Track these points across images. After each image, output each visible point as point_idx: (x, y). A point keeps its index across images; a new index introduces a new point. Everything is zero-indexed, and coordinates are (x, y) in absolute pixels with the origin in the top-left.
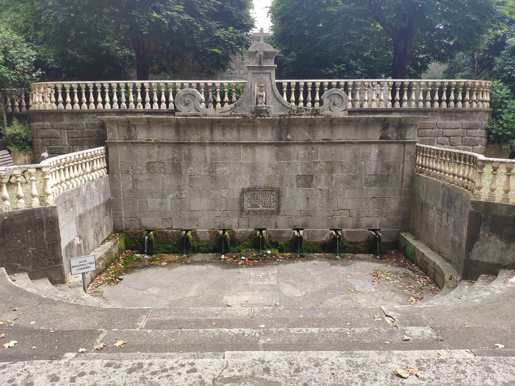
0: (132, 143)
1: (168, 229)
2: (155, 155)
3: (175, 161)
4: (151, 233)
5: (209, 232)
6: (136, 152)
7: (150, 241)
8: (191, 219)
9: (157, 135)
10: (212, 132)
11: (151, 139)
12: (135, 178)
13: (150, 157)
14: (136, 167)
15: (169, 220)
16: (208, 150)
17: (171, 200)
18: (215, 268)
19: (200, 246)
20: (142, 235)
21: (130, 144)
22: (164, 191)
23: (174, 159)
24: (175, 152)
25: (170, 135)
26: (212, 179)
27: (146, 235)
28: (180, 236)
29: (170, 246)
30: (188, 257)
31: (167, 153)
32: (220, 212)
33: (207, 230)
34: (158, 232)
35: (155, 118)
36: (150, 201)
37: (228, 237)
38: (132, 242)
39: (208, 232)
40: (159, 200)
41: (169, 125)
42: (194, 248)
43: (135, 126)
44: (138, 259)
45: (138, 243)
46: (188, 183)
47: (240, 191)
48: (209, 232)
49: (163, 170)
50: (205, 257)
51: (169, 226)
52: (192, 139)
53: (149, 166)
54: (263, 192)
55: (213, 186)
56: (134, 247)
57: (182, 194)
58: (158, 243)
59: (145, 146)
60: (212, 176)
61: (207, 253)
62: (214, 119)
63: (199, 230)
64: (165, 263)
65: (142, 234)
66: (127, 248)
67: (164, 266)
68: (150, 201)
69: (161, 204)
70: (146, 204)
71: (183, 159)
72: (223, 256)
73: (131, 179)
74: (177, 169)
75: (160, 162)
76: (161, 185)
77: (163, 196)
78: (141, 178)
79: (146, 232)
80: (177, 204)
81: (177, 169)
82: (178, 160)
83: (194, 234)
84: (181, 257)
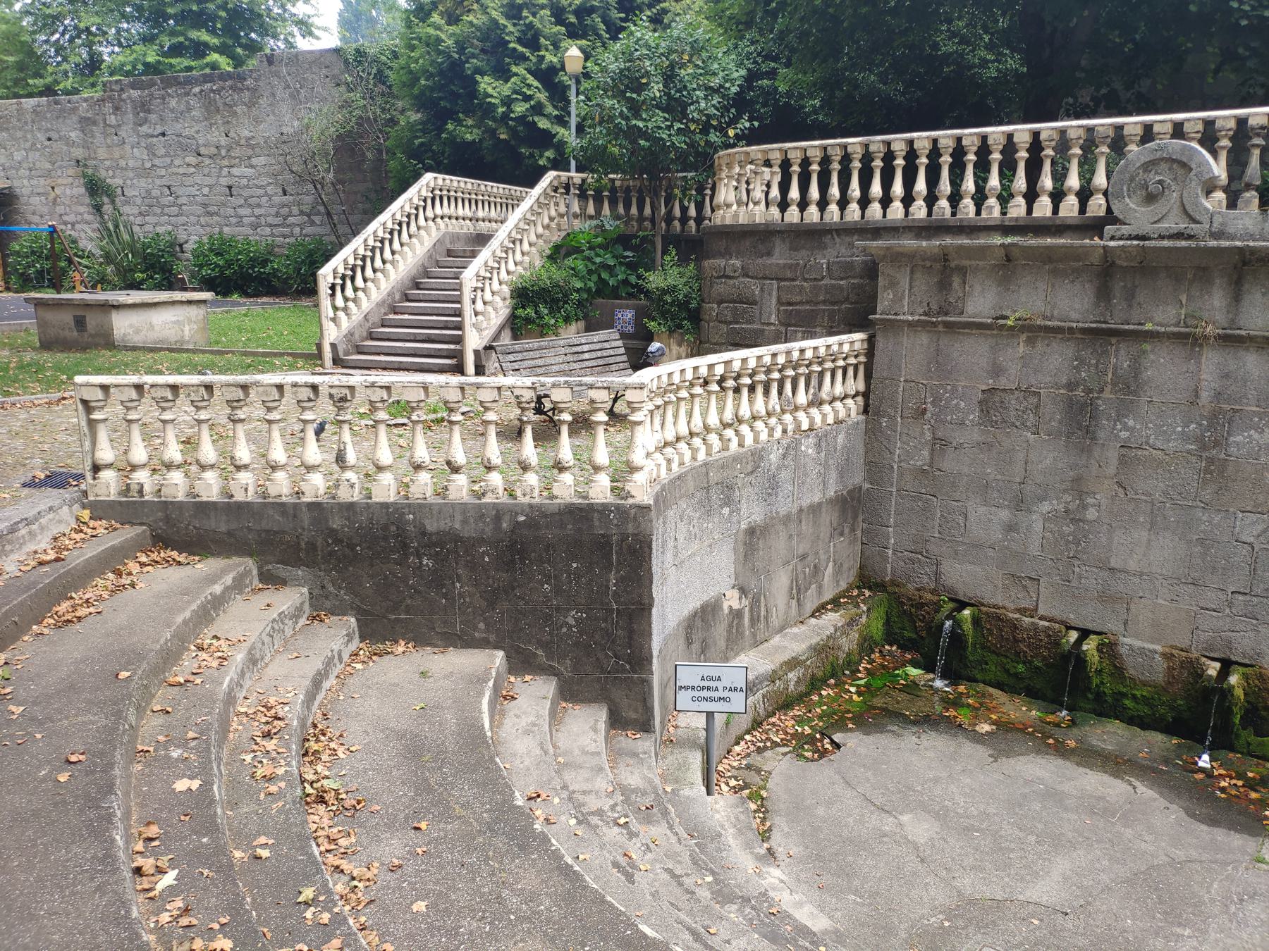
0: (947, 325)
2: (1014, 369)
3: (1079, 392)
4: (967, 612)
5: (1167, 657)
6: (955, 354)
7: (957, 638)
8: (1105, 598)
9: (1033, 299)
10: (1237, 298)
11: (1008, 313)
12: (940, 434)
13: (997, 371)
14: (948, 401)
16: (1211, 362)
17: (1046, 519)
18: (1162, 802)
19: (1124, 695)
20: (938, 611)
21: (940, 328)
23: (1077, 384)
24: (1082, 362)
25: (1072, 303)
26: (1207, 471)
27: (948, 618)
28: (1058, 644)
29: (1021, 668)
30: (1073, 723)
31: (1055, 362)
32: (1223, 597)
33: (1159, 648)
34: (987, 614)
35: (1030, 247)
36: (977, 511)
37: (1239, 692)
38: (907, 625)
39: (1163, 655)
40: (1004, 514)
41: (1075, 270)
42: (1099, 696)
43: (963, 271)
44: (912, 688)
45: (924, 634)
46: (1112, 470)
48: (1167, 657)
49: (1031, 419)
50: (1136, 744)
52: (1151, 320)
53: (990, 403)
55: (1207, 495)
56: (910, 640)
57: (1085, 507)
58: (983, 648)
59: (986, 336)
60: (1211, 461)
61: (1144, 726)
62: (1253, 251)
64: (985, 728)
65: (937, 607)
66: (890, 638)
67: (979, 739)
68: (977, 511)
69: (1011, 528)
70: (961, 520)
71: (1108, 389)
72: (1206, 757)
73: (928, 436)
74: (1081, 419)
75: (1028, 392)
76: (1018, 468)
77: (1020, 504)
78: (958, 437)
81: (1081, 419)
82: (1091, 391)
83: (1109, 649)
84: (1051, 718)
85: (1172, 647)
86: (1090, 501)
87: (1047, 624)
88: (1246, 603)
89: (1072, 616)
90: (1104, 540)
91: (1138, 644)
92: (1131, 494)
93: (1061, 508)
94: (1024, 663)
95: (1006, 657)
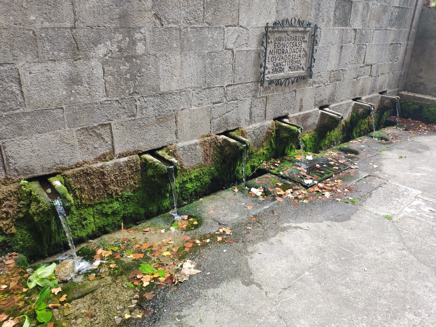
1: (103, 158)
5: (203, 144)
15: (101, 131)
17: (105, 63)
22: (81, 33)
29: (116, 205)
33: (196, 141)
34: (74, 176)
40: (63, 68)
45: (14, 230)
47: (258, 32)
51: (104, 150)
54: (293, 35)
57: (134, 43)
63: (180, 145)
68: (30, 70)
69: (73, 80)
70: (15, 88)
77: (76, 51)
80: (120, 74)
85: (203, 137)
86: (138, 36)
87: (126, 159)
88: (233, 91)
89: (141, 144)
90: (153, 70)
91: (186, 143)
92: (165, 23)
93: (115, 48)
94: (117, 200)
95: (101, 203)
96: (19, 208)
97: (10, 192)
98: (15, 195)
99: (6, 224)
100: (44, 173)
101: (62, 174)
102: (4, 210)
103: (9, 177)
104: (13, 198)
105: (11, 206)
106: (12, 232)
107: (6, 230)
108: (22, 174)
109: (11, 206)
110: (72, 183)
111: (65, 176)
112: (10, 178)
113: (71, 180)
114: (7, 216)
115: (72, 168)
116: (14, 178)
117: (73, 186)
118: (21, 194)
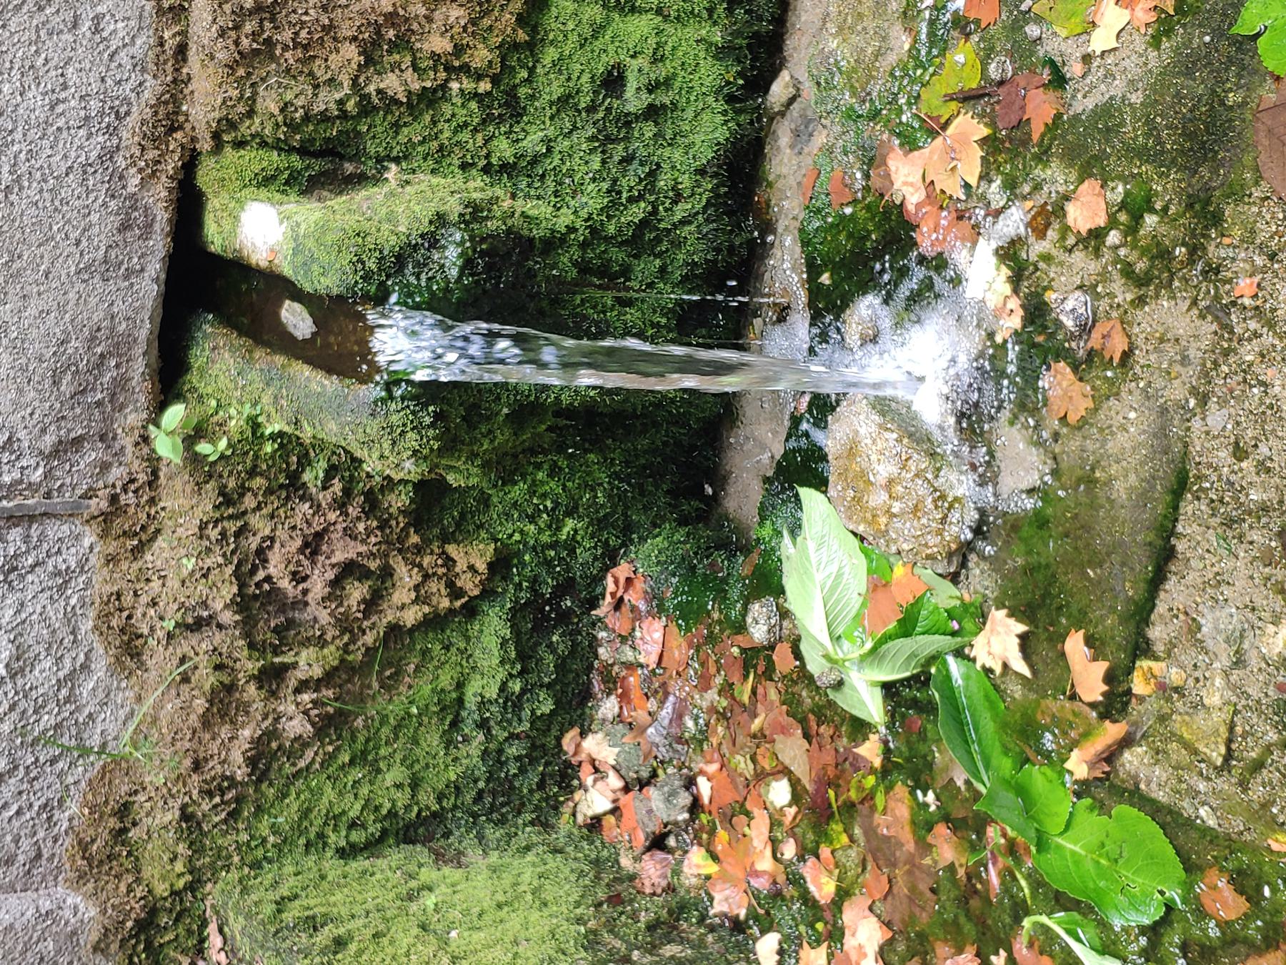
38: (421, 688)
45: (472, 557)
58: (507, 107)
66: (524, 786)
79: (219, 361)
96: (341, 504)
97: (214, 534)
98: (249, 502)
99: (417, 588)
100: (155, 267)
101: (205, 145)
102: (318, 586)
103: (99, 504)
104: (255, 521)
105: (313, 546)
106: (482, 567)
107: (455, 593)
108: (108, 420)
109: (313, 546)
110: (298, 94)
111: (225, 133)
112: (114, 499)
113: (269, 103)
114: (364, 574)
115: (182, 50)
116: (117, 474)
117: (326, 100)
118: (252, 473)
